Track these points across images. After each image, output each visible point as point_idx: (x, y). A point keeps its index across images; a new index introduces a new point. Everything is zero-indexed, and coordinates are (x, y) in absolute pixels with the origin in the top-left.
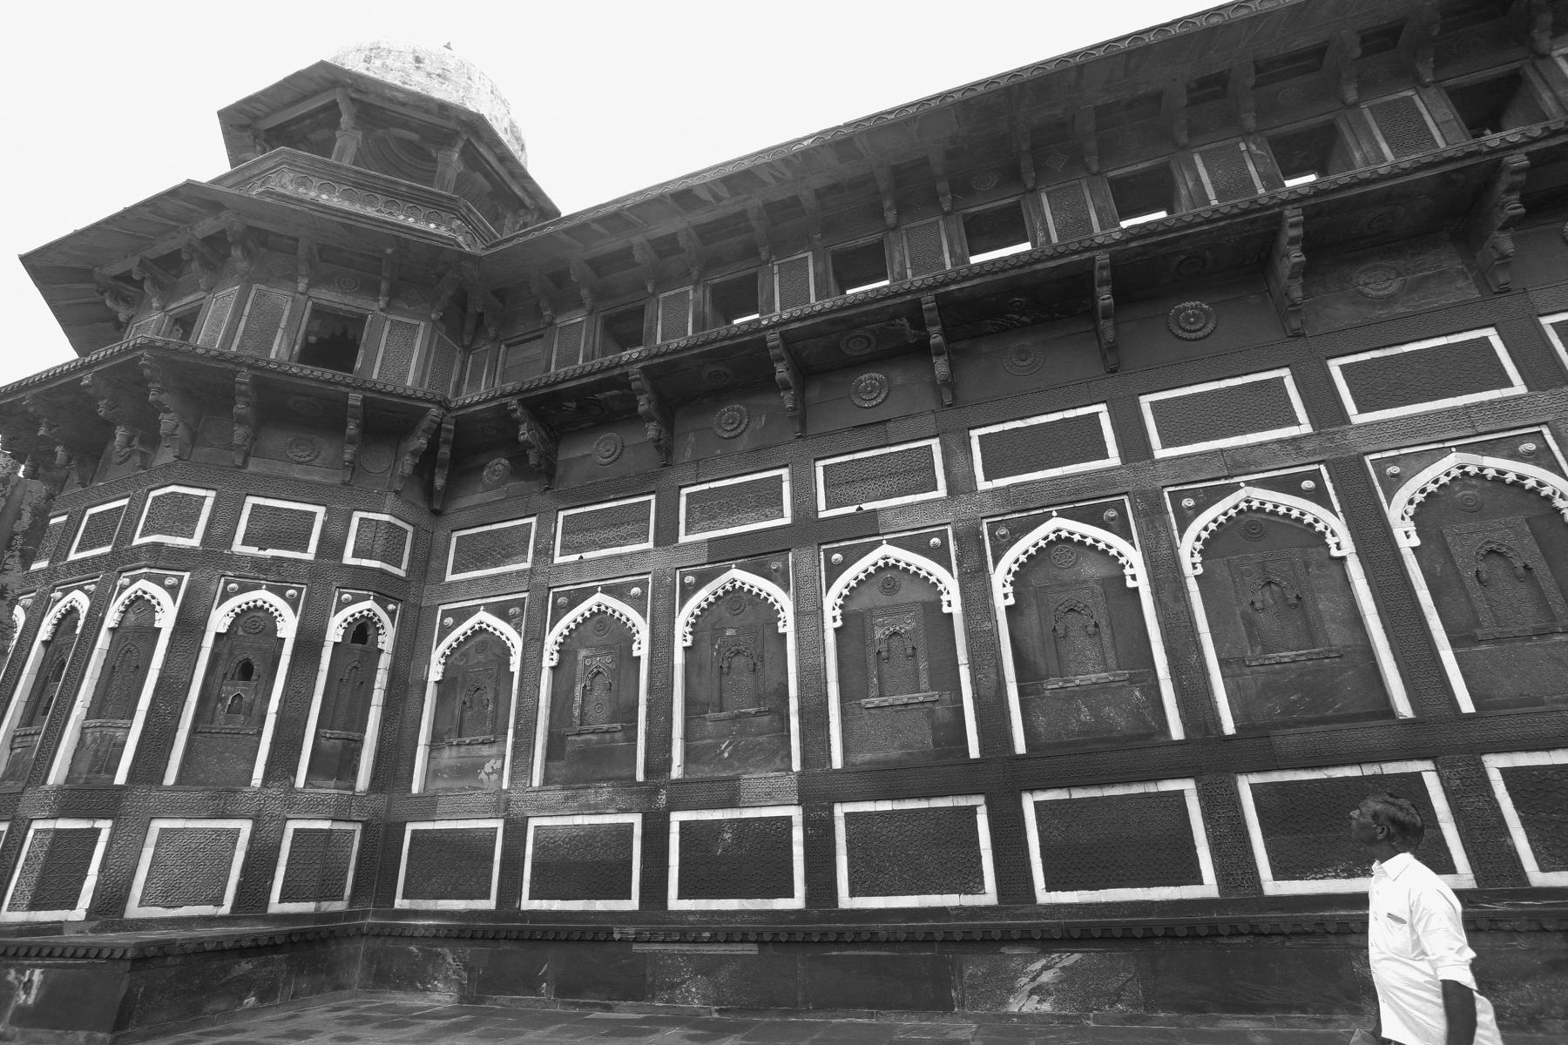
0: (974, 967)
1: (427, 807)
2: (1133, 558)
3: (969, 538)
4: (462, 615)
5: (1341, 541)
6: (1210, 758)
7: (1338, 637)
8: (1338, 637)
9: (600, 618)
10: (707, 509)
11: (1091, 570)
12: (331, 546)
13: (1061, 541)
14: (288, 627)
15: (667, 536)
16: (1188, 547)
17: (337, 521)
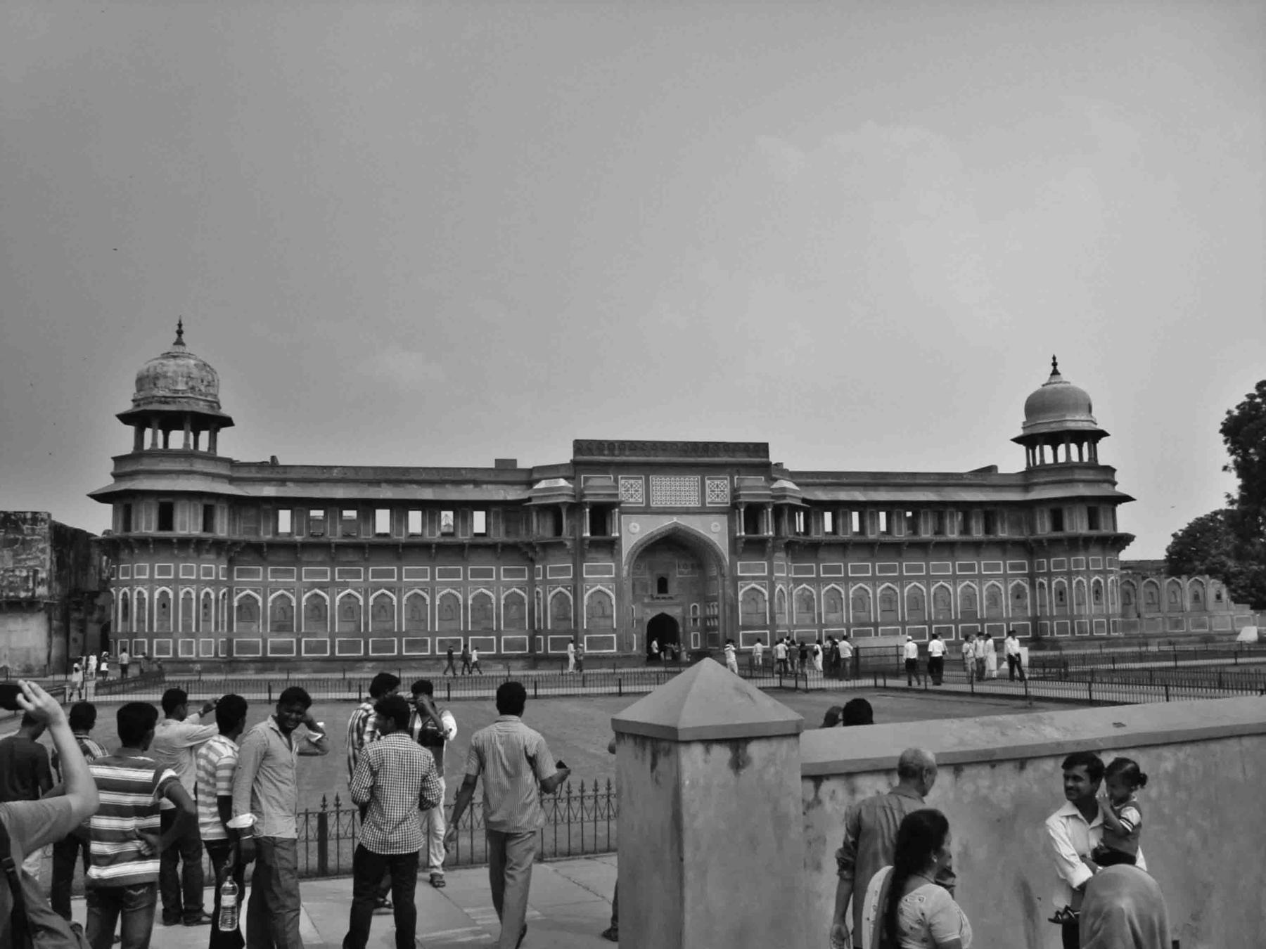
0: (359, 665)
1: (239, 635)
2: (395, 599)
3: (366, 591)
4: (242, 590)
5: (428, 601)
6: (400, 635)
7: (423, 616)
8: (423, 616)
9: (282, 595)
10: (309, 574)
11: (387, 600)
12: (217, 574)
13: (383, 594)
14: (213, 597)
15: (299, 578)
16: (405, 598)
17: (217, 567)
